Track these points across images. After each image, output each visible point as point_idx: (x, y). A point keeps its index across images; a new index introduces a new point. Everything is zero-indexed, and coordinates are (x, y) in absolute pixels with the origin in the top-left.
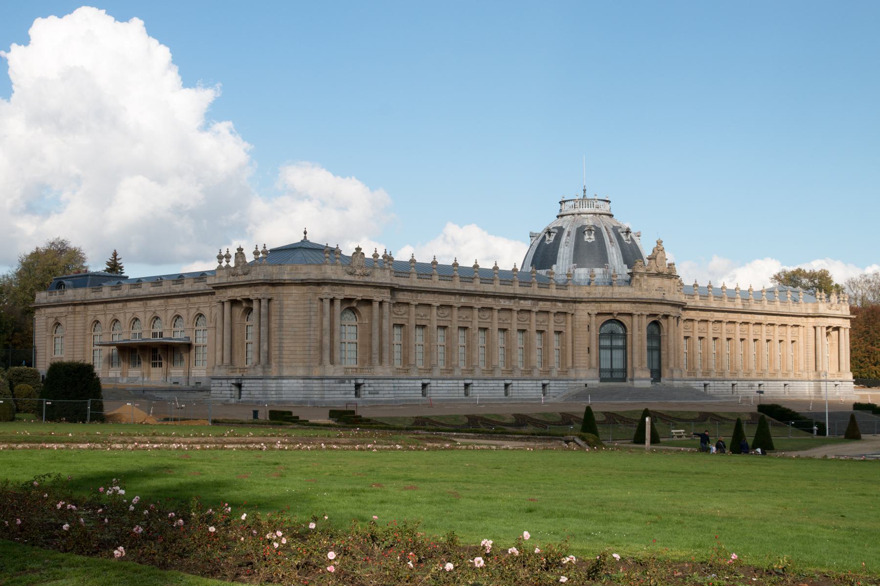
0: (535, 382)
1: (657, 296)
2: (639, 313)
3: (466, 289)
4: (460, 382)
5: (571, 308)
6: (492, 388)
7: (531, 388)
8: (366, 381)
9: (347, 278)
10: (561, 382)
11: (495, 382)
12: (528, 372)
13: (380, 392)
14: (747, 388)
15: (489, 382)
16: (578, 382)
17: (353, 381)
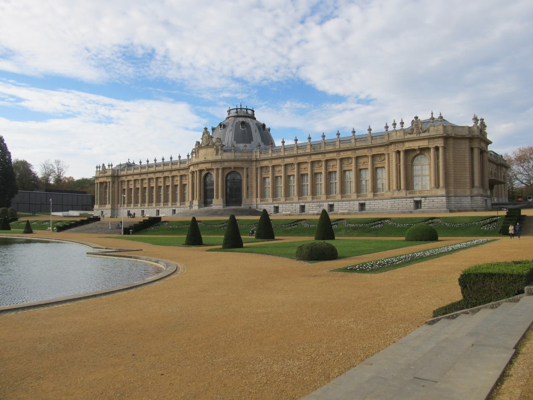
4: (140, 210)
8: (104, 210)
9: (101, 175)
13: (108, 214)
14: (315, 207)
17: (100, 210)
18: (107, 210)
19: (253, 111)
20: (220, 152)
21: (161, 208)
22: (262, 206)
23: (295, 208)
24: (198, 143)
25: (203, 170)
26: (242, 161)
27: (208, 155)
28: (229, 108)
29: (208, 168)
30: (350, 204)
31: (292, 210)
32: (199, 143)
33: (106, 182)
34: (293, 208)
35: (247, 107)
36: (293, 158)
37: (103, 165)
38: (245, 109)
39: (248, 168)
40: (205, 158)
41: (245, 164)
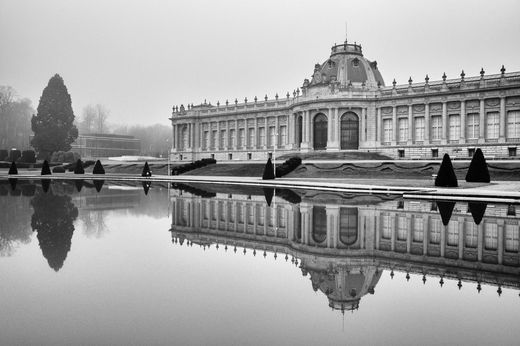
0: (264, 152)
1: (314, 98)
3: (230, 112)
4: (226, 153)
5: (287, 113)
6: (241, 156)
7: (261, 155)
8: (183, 154)
9: (179, 116)
10: (279, 152)
11: (243, 153)
12: (259, 147)
14: (451, 152)
15: (240, 153)
16: (288, 152)
17: (179, 154)
18: (188, 154)
19: (361, 48)
20: (336, 91)
21: (253, 152)
22: (383, 149)
23: (425, 152)
24: (306, 81)
25: (315, 110)
26: (362, 101)
27: (321, 94)
28: (335, 44)
30: (496, 149)
31: (422, 154)
32: (308, 80)
33: (186, 124)
34: (423, 152)
35: (355, 43)
36: (423, 99)
37: (182, 105)
38: (353, 45)
39: (366, 109)
40: (317, 97)
41: (364, 105)
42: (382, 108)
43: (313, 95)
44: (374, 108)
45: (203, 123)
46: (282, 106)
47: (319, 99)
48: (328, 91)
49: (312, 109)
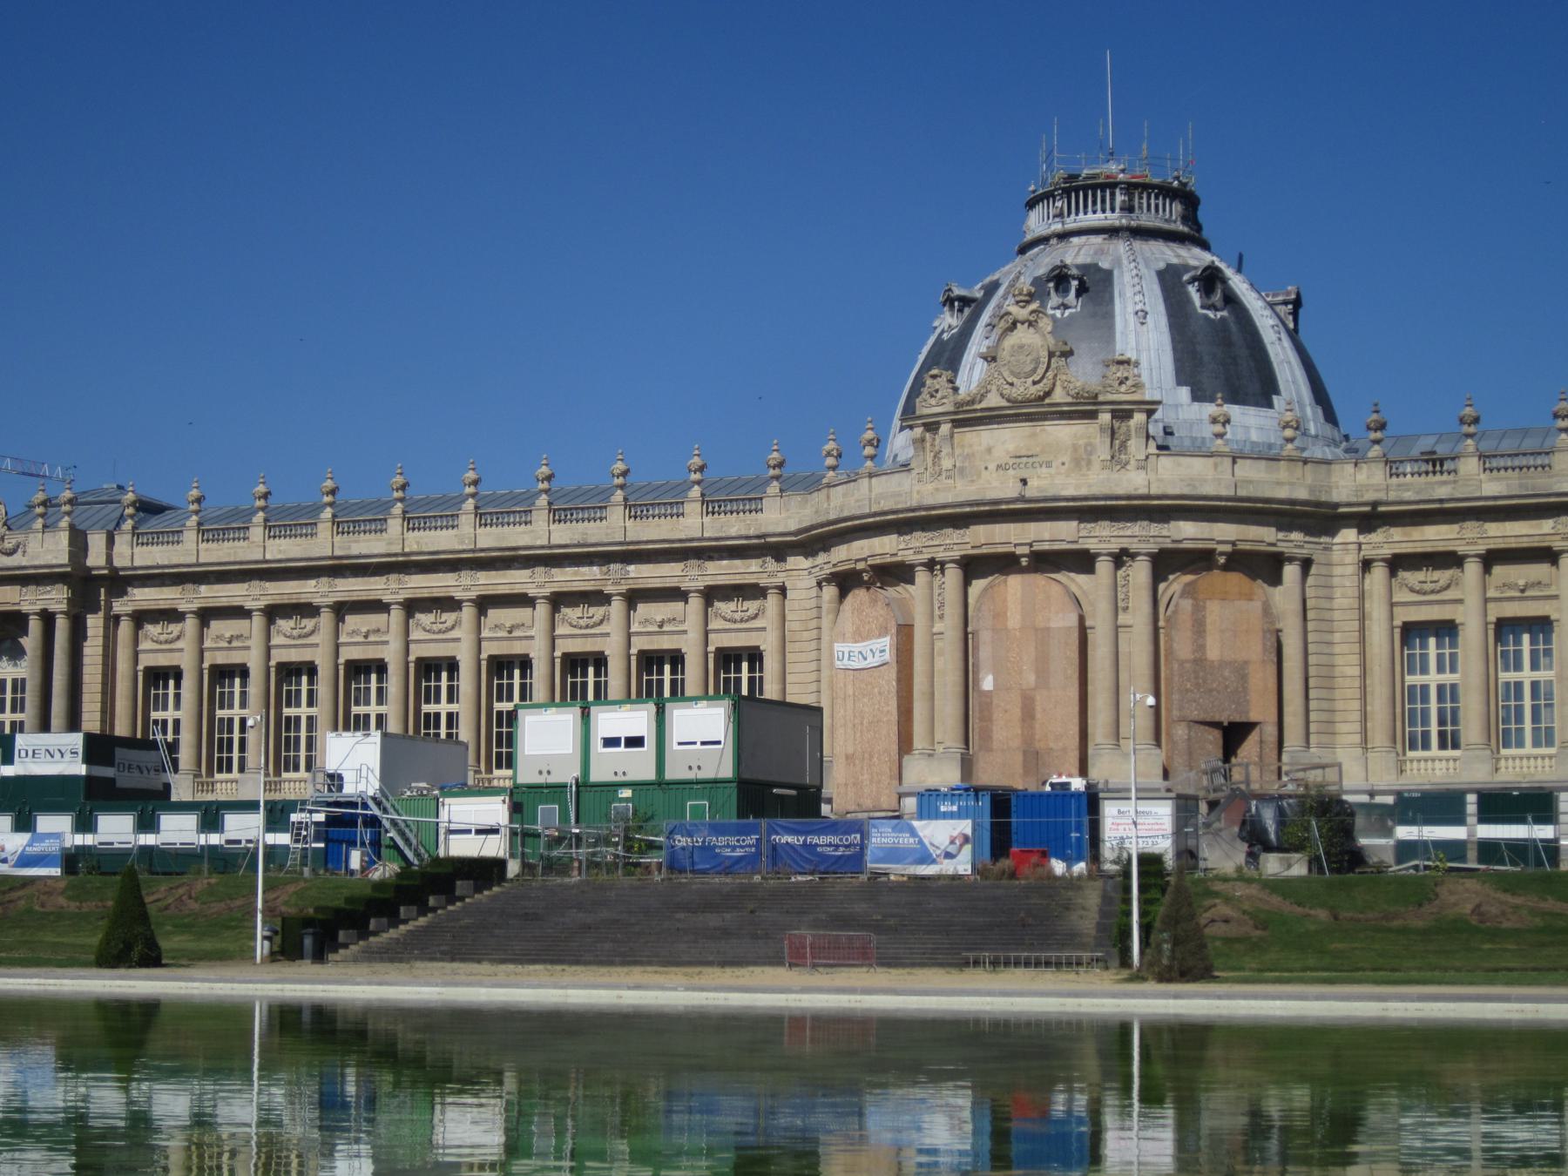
1: (1001, 487)
2: (925, 557)
20: (1136, 447)
29: (1036, 547)
39: (1306, 564)
40: (1024, 482)
42: (1397, 563)
43: (992, 466)
44: (1352, 558)
45: (141, 618)
46: (734, 527)
47: (1030, 492)
48: (1090, 449)
49: (984, 550)
